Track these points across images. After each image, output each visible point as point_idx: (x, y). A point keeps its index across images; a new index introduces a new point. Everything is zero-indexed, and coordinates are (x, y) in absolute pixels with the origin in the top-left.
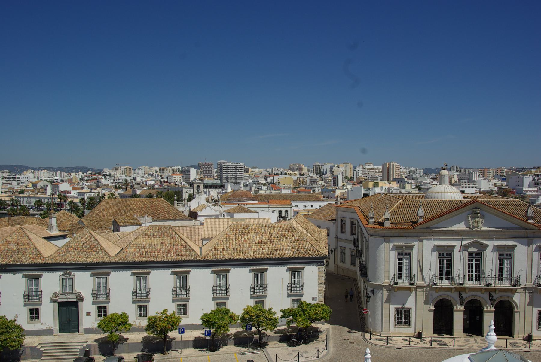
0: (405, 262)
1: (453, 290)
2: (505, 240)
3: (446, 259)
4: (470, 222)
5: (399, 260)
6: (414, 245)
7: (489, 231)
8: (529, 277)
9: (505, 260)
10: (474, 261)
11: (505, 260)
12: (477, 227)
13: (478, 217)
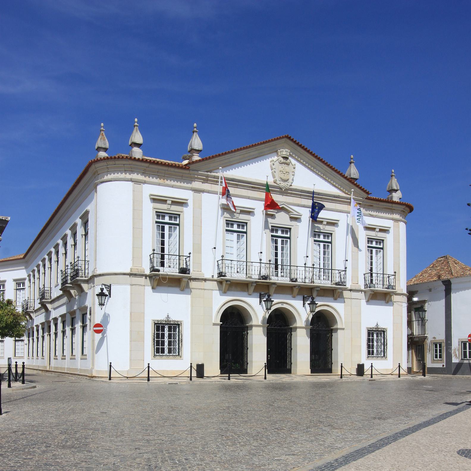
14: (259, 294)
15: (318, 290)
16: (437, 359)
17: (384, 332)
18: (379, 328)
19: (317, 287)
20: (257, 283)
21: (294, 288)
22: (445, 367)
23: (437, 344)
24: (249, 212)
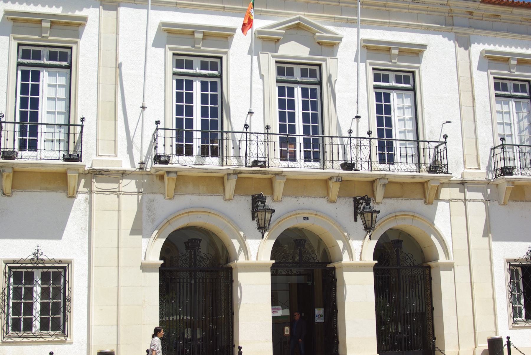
0: (49, 85)
1: (231, 185)
2: (390, 27)
3: (202, 82)
5: (25, 76)
6: (85, 19)
8: (470, 151)
9: (393, 95)
10: (298, 91)
11: (395, 95)
14: (251, 198)
15: (385, 185)
19: (380, 179)
20: (240, 175)
21: (329, 181)
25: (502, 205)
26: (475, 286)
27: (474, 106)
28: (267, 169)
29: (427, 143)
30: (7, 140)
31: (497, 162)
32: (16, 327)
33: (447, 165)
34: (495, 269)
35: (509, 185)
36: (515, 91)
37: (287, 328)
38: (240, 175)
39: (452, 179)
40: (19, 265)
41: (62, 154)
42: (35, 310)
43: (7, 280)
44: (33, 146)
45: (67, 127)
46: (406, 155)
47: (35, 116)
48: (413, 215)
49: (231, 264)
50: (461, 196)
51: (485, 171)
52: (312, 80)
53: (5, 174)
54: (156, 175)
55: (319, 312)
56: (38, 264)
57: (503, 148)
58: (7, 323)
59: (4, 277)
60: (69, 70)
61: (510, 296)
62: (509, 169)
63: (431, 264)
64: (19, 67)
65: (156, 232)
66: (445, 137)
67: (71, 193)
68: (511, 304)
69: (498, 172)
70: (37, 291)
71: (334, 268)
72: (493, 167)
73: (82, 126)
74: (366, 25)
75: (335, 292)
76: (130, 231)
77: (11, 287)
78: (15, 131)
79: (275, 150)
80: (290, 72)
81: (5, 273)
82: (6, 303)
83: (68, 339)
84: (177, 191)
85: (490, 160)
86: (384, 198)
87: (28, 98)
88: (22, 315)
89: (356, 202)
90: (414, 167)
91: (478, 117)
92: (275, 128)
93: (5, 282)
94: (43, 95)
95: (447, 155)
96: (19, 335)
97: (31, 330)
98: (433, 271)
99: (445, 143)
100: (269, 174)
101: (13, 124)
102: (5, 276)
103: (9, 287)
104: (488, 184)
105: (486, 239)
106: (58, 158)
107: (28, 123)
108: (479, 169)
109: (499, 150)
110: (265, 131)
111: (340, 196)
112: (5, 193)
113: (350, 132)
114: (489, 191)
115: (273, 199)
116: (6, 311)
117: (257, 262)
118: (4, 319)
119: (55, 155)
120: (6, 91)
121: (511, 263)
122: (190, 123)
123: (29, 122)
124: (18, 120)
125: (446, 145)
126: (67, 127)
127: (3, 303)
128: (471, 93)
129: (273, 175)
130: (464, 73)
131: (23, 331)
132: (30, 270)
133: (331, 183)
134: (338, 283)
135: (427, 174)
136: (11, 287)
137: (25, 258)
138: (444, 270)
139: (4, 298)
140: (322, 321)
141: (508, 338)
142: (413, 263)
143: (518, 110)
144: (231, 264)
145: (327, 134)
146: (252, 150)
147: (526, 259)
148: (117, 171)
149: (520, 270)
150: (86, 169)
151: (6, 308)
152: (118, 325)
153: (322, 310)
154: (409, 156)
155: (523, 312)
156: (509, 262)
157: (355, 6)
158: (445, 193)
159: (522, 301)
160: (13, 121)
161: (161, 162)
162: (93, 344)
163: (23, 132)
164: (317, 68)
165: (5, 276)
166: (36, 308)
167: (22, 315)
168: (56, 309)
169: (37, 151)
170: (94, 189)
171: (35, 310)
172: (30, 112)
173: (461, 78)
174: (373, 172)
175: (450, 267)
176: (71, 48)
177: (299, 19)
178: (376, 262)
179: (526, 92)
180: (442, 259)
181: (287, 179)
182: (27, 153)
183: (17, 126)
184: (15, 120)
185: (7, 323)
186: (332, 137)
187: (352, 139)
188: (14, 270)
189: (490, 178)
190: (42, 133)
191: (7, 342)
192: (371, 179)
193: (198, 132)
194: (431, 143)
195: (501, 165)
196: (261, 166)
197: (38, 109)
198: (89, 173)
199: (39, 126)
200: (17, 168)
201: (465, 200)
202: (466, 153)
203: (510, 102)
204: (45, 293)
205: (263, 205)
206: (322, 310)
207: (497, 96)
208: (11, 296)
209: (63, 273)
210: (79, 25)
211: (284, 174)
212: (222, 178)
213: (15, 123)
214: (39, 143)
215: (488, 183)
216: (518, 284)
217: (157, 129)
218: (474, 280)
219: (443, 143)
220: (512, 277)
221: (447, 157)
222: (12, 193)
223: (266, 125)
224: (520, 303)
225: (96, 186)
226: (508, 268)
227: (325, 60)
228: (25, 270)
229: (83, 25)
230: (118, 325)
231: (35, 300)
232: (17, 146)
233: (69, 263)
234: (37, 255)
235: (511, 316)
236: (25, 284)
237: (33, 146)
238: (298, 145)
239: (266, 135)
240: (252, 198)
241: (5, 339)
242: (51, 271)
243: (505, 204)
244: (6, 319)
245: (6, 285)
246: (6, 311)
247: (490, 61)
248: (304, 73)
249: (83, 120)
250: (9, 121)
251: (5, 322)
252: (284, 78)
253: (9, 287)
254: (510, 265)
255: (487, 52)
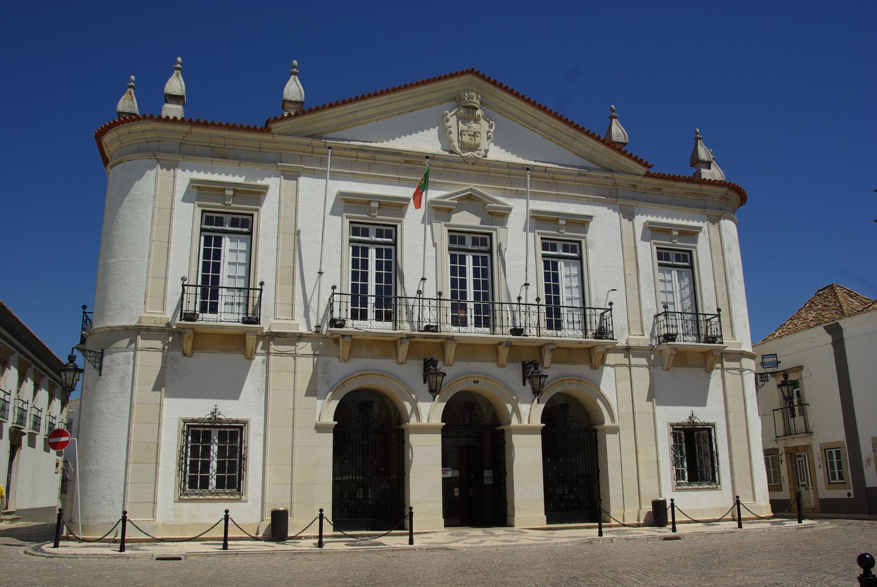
0: (231, 251)
1: (403, 349)
2: (557, 198)
3: (377, 249)
4: (450, 133)
5: (208, 241)
6: (266, 188)
7: (510, 166)
9: (561, 264)
10: (469, 259)
11: (562, 263)
12: (475, 148)
13: (476, 120)
14: (423, 361)
15: (552, 350)
16: (835, 482)
17: (709, 430)
18: (697, 424)
19: (548, 344)
22: (852, 496)
23: (830, 453)
24: (398, 206)
25: (665, 370)
26: (639, 449)
27: (638, 275)
28: (438, 334)
29: (593, 310)
30: (189, 302)
31: (661, 328)
32: (193, 485)
33: (613, 331)
34: (659, 433)
35: (672, 351)
36: (677, 261)
37: (456, 489)
38: (412, 340)
39: (617, 345)
40: (198, 424)
41: (241, 317)
42: (212, 468)
43: (185, 438)
44: (214, 309)
45: (247, 290)
46: (573, 321)
47: (216, 280)
48: (580, 380)
49: (403, 426)
50: (626, 361)
51: (649, 337)
52: (483, 248)
53: (186, 336)
54: (332, 338)
55: (488, 473)
56: (215, 423)
57: (666, 315)
58: (185, 481)
59: (183, 435)
60: (250, 236)
61: (673, 459)
62: (672, 335)
63: (598, 427)
64: (202, 232)
65: (330, 393)
66: (611, 304)
67: (249, 354)
68: (674, 467)
69: (661, 338)
70: (214, 449)
71: (503, 431)
72: (656, 334)
73: (261, 290)
74: (535, 196)
75: (504, 454)
76: (305, 392)
77: (189, 445)
78: (196, 294)
79: (446, 315)
80: (462, 241)
81: (183, 432)
82: (184, 461)
83: (243, 497)
84: (351, 354)
85: (654, 326)
86: (552, 362)
87: (210, 262)
88: (199, 473)
89: (525, 367)
90: (581, 333)
91: (642, 285)
92: (447, 294)
93: (184, 440)
94: (224, 259)
95: (612, 322)
96: (196, 492)
97: (207, 488)
98: (598, 433)
99: (611, 310)
100: (440, 338)
101: (195, 287)
102: (184, 434)
103: (187, 445)
104: (652, 350)
105: (651, 403)
106: (237, 321)
107: (210, 287)
108: (643, 335)
109: (662, 318)
110: (437, 297)
111: (509, 361)
112: (185, 353)
113: (519, 298)
114: (653, 356)
115: (444, 363)
116: (183, 469)
117: (428, 424)
118: (182, 476)
119: (235, 318)
120: (189, 255)
121: (675, 427)
122: (365, 288)
123: (210, 285)
124: (200, 283)
125: (611, 312)
126: (247, 290)
127: (181, 461)
128: (635, 263)
129: (445, 340)
130: (629, 243)
131: (200, 488)
132: (207, 429)
133: (501, 348)
134: (507, 446)
135: (593, 340)
136: (189, 445)
137: (203, 417)
138: (609, 433)
139: (181, 456)
140: (491, 482)
141: (672, 500)
142: (580, 426)
143: (680, 279)
144: (403, 426)
145: (497, 300)
146: (425, 315)
147: (689, 422)
148: (294, 334)
149: (683, 433)
150: (264, 331)
151: (183, 465)
152: (292, 484)
153: (491, 471)
154: (576, 323)
155: (686, 474)
156: (672, 425)
157: (524, 178)
158: (611, 358)
159: (685, 464)
160: (195, 284)
161: (337, 326)
162: (267, 502)
163: (204, 295)
164: (488, 237)
165: (184, 434)
166: (213, 466)
167: (199, 473)
168: (232, 467)
169: (217, 314)
170: (272, 351)
171: (212, 468)
172: (212, 275)
173: (625, 248)
174: (541, 338)
175: (615, 430)
176: (252, 215)
177: (471, 189)
178: (544, 425)
179: (687, 262)
180: (608, 422)
181: (458, 344)
182: (208, 316)
183: (199, 289)
184: (197, 283)
185: (185, 481)
186: (502, 303)
187: (521, 305)
188: (192, 429)
189: (654, 344)
190: (223, 297)
191: (184, 499)
192: (539, 344)
193: (372, 297)
194: (597, 310)
195: (664, 331)
196: (433, 331)
197: (219, 273)
198: (267, 335)
199: (220, 290)
200: (198, 330)
201: (630, 366)
202: (630, 319)
203: (673, 271)
204: (221, 451)
205: (435, 368)
206: (491, 471)
207: (660, 265)
208: (189, 454)
209: (239, 433)
210: (261, 193)
211: (455, 338)
212: (396, 342)
213: (197, 286)
214: (219, 306)
215: (651, 349)
216: (681, 447)
217: (333, 294)
218: (639, 443)
219: (608, 310)
220: (675, 441)
221: (612, 324)
222: (192, 353)
223: (438, 291)
224: (683, 466)
225: (273, 348)
226: (672, 431)
227: (495, 230)
228: (203, 429)
229: (265, 194)
230: (292, 484)
231: (212, 459)
232: (198, 309)
233: (246, 423)
234: (214, 414)
235: (674, 479)
236: (203, 442)
237: (214, 309)
238: (469, 311)
239: (439, 301)
240: (425, 363)
241: (182, 496)
242: (228, 430)
243: (668, 370)
244: (183, 476)
245: (185, 443)
246: (183, 469)
247: (653, 232)
248: (475, 242)
249: (262, 284)
250: (191, 284)
251: (183, 479)
252: (455, 246)
253: (187, 445)
254: (674, 429)
255: (650, 223)
